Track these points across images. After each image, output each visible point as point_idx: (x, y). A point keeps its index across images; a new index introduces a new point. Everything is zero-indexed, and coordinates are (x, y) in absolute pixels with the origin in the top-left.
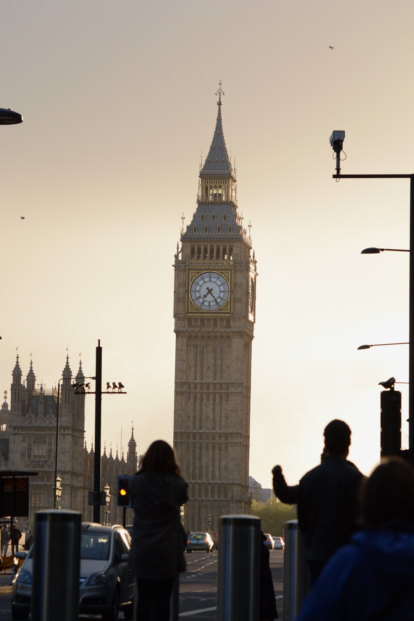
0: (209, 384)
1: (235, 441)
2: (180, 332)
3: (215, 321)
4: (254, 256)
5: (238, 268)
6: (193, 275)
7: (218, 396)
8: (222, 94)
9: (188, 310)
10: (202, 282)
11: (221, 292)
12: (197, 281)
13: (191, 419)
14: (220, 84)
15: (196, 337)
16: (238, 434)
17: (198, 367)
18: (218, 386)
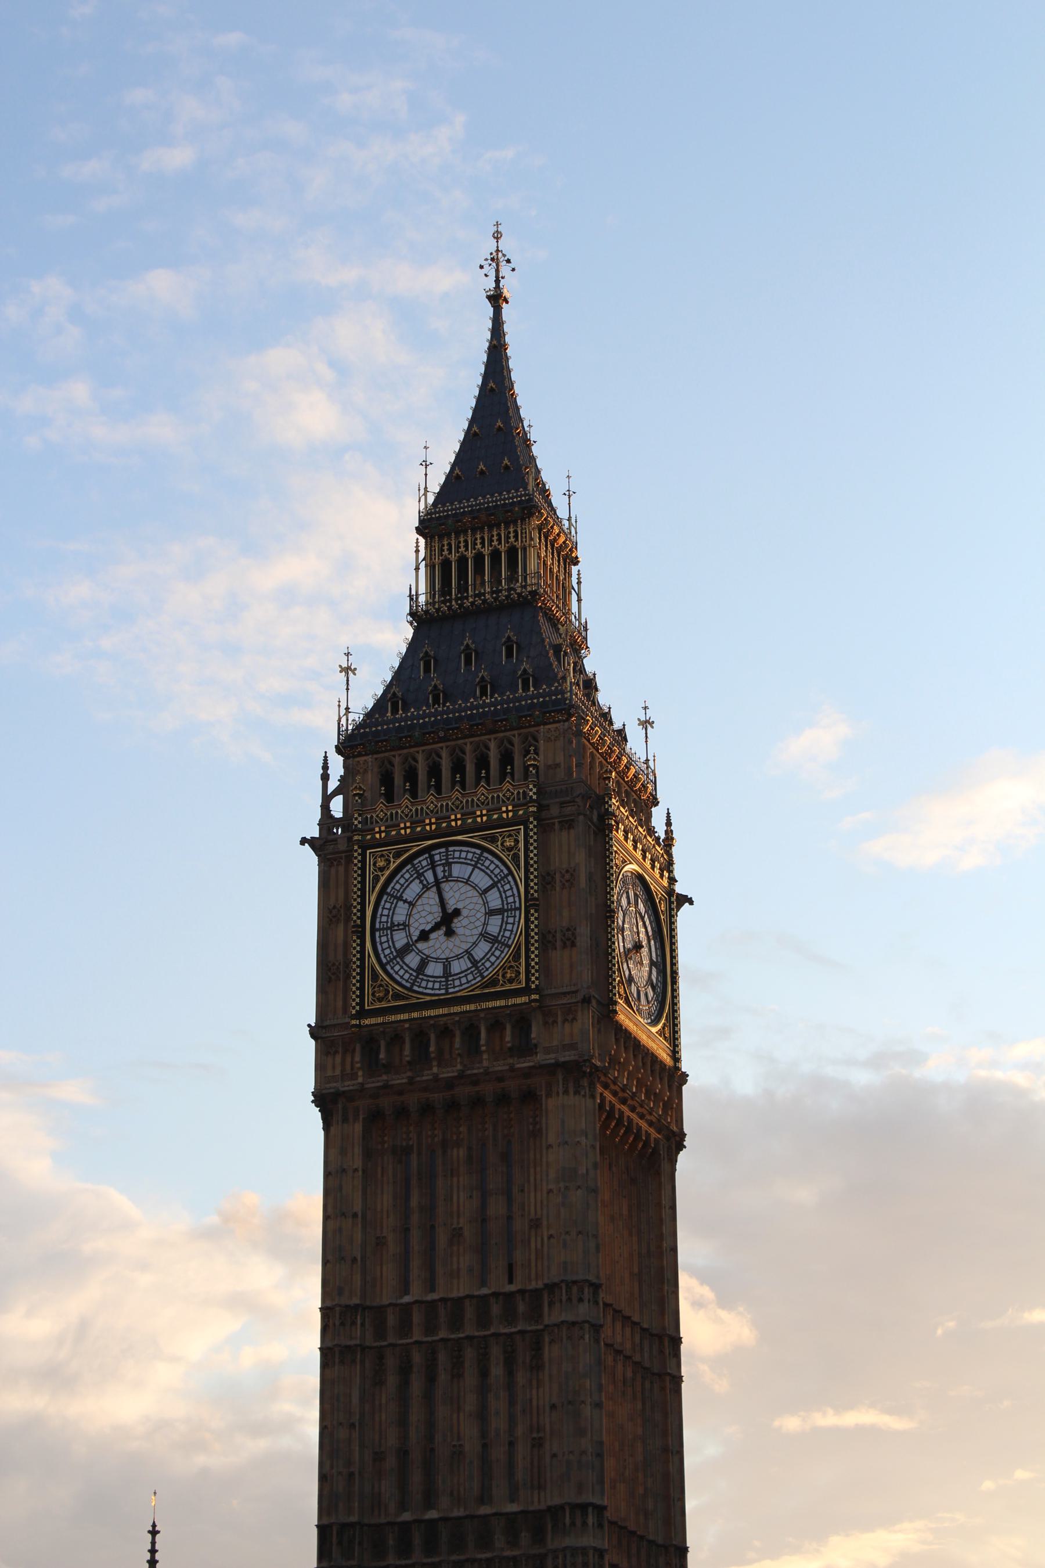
0: (459, 1301)
1: (569, 1541)
2: (337, 1095)
3: (471, 1031)
4: (669, 833)
5: (555, 811)
6: (381, 863)
7: (496, 1352)
8: (505, 270)
9: (361, 1004)
10: (416, 887)
11: (491, 913)
12: (395, 886)
13: (391, 1462)
14: (497, 236)
15: (402, 1112)
16: (583, 1507)
17: (415, 1236)
18: (496, 1309)
